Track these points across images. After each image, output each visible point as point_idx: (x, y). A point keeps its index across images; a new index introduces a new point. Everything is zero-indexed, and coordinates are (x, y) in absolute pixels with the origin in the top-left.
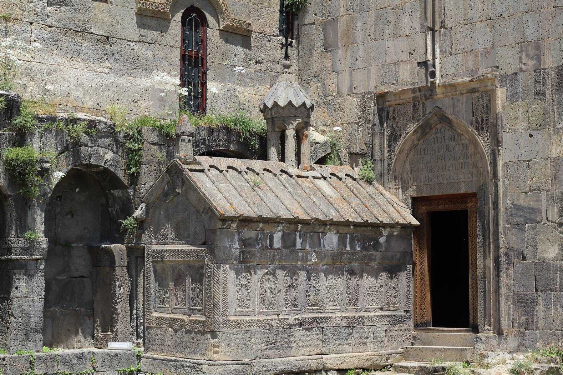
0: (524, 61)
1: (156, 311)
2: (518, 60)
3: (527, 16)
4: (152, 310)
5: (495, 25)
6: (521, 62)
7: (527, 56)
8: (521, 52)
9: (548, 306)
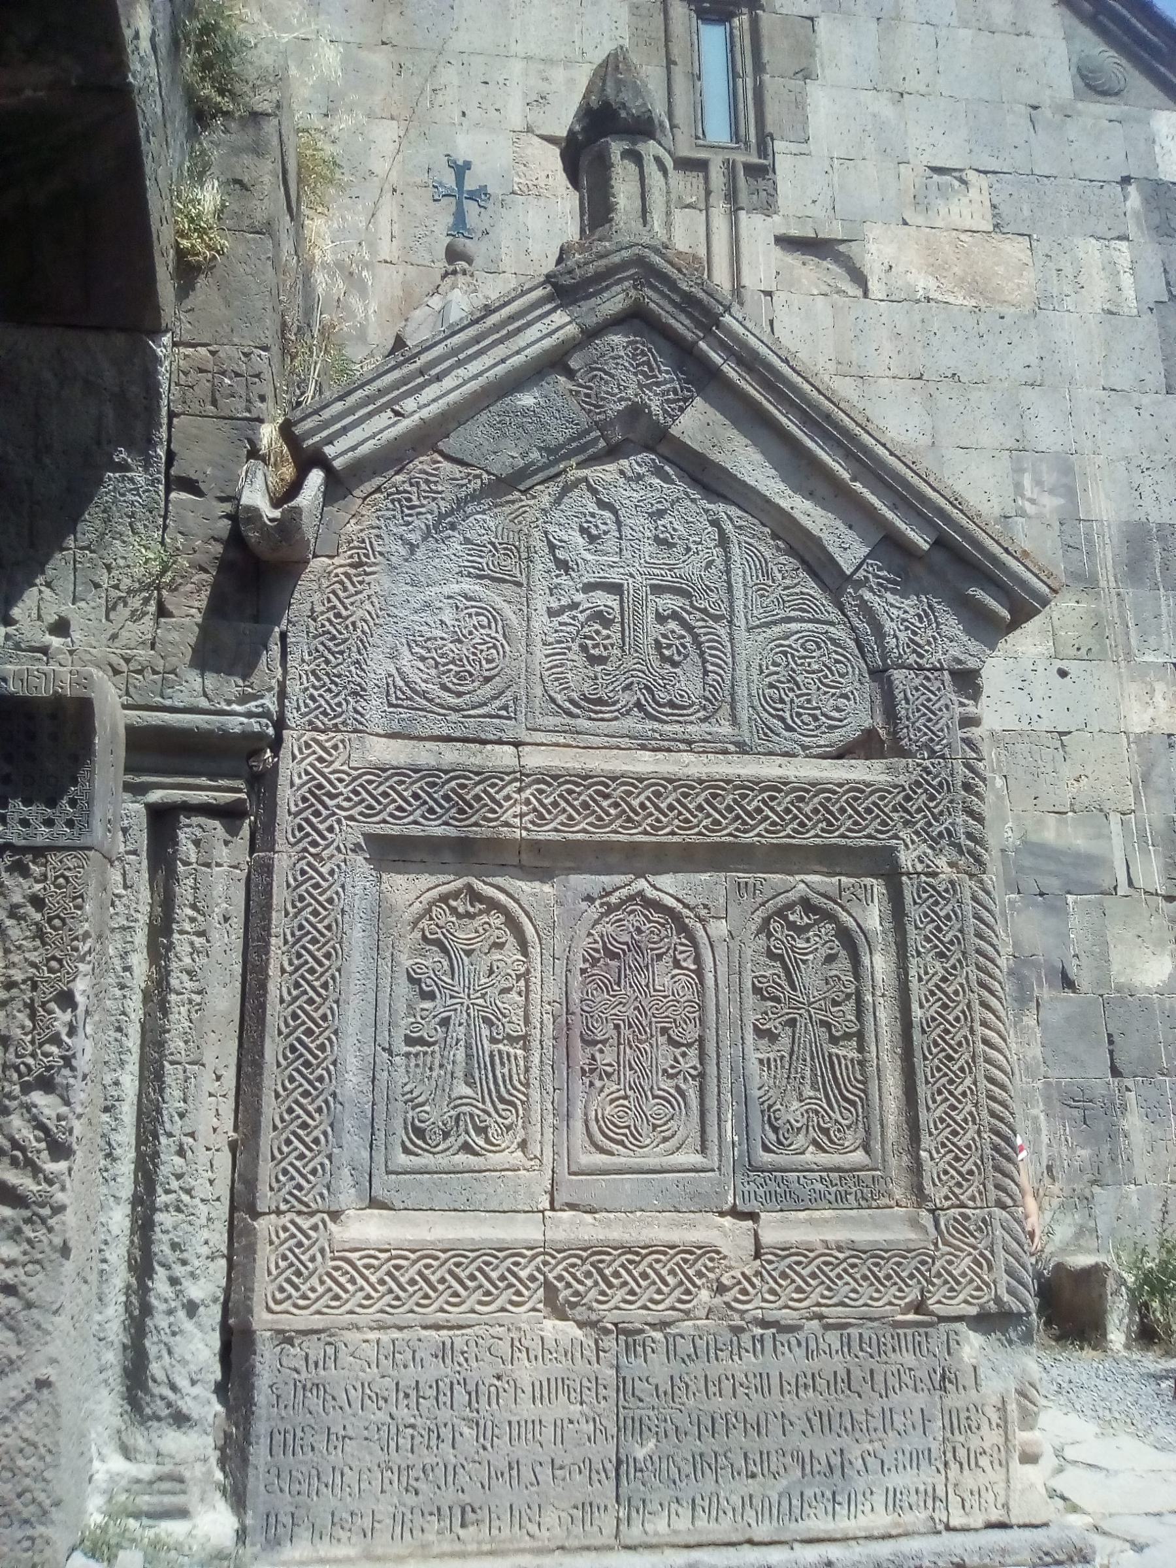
0: (1028, 494)
1: (374, 1203)
2: (1012, 488)
3: (1029, 396)
4: (347, 1196)
5: (936, 394)
6: (1023, 496)
7: (1038, 483)
9: (1154, 1114)
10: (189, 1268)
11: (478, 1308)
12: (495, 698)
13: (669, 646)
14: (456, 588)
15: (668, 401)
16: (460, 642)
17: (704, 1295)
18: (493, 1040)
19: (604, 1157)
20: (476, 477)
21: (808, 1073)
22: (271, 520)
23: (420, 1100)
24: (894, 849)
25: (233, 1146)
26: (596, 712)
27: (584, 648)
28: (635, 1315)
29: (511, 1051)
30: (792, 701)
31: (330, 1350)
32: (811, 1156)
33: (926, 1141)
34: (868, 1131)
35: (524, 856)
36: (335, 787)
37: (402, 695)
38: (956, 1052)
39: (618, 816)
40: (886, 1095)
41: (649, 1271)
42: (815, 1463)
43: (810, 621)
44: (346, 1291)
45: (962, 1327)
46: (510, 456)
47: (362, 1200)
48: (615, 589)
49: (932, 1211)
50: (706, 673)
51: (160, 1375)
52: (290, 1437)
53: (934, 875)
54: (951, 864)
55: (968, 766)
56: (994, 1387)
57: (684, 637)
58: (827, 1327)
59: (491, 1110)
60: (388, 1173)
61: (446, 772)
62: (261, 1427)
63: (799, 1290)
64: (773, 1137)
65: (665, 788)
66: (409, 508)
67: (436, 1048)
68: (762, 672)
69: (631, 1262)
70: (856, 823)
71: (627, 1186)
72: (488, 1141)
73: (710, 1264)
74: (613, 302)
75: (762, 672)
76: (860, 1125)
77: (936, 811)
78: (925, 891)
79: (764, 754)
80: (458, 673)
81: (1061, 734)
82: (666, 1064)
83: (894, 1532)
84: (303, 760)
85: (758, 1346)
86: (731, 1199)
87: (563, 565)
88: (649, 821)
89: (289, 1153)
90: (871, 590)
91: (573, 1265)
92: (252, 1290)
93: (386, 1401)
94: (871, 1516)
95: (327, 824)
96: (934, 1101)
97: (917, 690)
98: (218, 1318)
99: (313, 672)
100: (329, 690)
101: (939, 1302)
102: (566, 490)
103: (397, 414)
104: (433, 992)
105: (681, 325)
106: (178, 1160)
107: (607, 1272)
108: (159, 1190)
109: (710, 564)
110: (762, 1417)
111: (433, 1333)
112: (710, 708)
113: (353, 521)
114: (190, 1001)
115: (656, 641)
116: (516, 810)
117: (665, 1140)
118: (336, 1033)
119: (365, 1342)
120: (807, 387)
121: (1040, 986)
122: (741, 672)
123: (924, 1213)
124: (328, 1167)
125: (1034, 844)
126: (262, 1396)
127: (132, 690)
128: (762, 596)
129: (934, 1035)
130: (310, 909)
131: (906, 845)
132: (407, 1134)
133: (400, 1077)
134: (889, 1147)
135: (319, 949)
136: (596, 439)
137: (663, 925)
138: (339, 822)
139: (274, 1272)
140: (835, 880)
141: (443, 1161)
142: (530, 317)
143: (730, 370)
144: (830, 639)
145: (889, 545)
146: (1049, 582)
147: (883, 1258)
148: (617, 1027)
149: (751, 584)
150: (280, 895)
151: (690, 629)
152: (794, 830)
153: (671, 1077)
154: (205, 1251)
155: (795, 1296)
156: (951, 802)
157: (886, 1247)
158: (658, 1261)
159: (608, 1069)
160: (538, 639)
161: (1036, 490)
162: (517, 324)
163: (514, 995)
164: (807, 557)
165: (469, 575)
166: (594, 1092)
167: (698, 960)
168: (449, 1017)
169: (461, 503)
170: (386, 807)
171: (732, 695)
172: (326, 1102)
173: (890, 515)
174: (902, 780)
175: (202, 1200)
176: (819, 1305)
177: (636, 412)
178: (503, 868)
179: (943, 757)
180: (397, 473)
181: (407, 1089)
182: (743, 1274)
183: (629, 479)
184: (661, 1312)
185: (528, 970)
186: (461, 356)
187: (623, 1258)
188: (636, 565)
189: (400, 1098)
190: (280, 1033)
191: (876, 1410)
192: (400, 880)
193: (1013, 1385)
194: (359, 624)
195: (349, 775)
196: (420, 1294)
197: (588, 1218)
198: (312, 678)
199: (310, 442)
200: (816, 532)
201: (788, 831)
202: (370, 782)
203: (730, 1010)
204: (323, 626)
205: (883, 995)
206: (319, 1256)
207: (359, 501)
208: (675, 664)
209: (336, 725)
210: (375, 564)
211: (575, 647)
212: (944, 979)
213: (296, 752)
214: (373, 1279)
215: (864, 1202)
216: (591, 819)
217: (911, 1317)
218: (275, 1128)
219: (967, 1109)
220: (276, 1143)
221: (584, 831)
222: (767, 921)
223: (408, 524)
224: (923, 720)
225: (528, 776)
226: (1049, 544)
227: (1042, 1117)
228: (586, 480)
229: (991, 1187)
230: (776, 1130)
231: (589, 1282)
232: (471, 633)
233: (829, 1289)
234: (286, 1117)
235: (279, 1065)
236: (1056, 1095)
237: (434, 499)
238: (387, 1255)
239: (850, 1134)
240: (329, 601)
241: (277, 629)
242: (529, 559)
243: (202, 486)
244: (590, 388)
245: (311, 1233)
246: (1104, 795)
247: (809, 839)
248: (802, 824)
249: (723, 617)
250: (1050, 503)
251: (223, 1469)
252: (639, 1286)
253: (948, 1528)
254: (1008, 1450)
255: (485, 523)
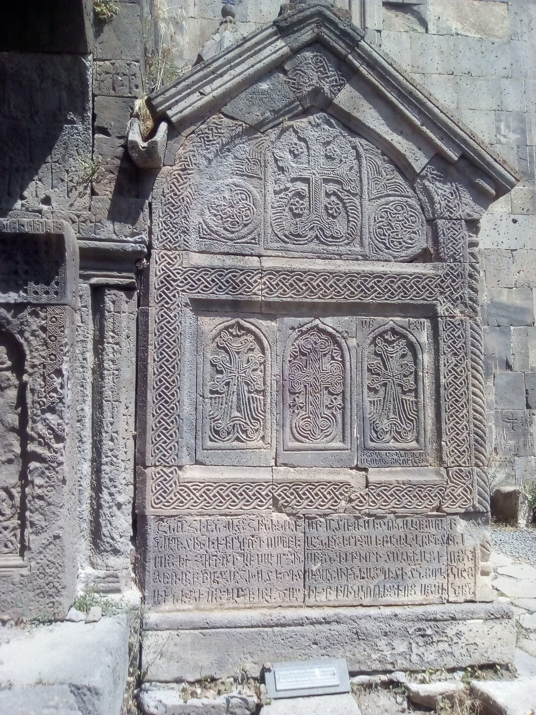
0: (503, 133)
1: (197, 462)
2: (495, 129)
3: (505, 83)
4: (185, 459)
5: (460, 82)
6: (500, 134)
7: (508, 127)
8: (499, 121)
10: (117, 489)
11: (244, 507)
12: (249, 234)
13: (332, 209)
14: (230, 181)
15: (333, 86)
16: (233, 207)
17: (343, 503)
18: (249, 392)
19: (299, 444)
20: (241, 125)
21: (392, 407)
22: (143, 148)
23: (217, 418)
24: (435, 305)
25: (135, 437)
26: (297, 241)
27: (291, 210)
28: (312, 511)
29: (257, 396)
30: (389, 235)
31: (180, 524)
32: (392, 444)
33: (444, 438)
34: (418, 433)
35: (263, 309)
36: (176, 277)
37: (206, 233)
38: (460, 398)
39: (307, 290)
40: (427, 417)
41: (319, 492)
42: (390, 573)
43: (399, 196)
44: (186, 499)
45: (457, 517)
46: (256, 115)
47: (192, 461)
48: (306, 180)
49: (446, 468)
50: (349, 221)
51: (107, 533)
52: (163, 560)
53: (453, 317)
54: (461, 312)
55: (471, 266)
56: (470, 543)
57: (338, 204)
58: (397, 517)
59: (249, 423)
60: (203, 449)
61: (227, 269)
62: (151, 555)
63: (385, 501)
64: (375, 435)
65: (329, 277)
66: (208, 141)
67: (224, 395)
68: (375, 221)
69: (311, 489)
70: (418, 293)
71: (309, 456)
72: (247, 436)
73: (346, 490)
74: (306, 35)
75: (375, 221)
76: (415, 430)
77: (455, 287)
78: (449, 325)
79: (375, 261)
80: (232, 222)
81: (512, 250)
82: (327, 403)
83: (424, 603)
84: (161, 264)
85: (367, 525)
86: (355, 462)
87: (281, 169)
88: (321, 292)
89: (159, 441)
90: (429, 180)
91: (285, 490)
92: (145, 498)
93: (204, 545)
94: (415, 596)
95: (172, 294)
96: (449, 420)
97: (449, 229)
98: (131, 510)
99: (165, 222)
100: (172, 231)
101: (448, 507)
102: (283, 131)
103: (202, 94)
104: (222, 371)
105: (340, 46)
106: (111, 443)
107: (300, 493)
108: (103, 456)
109: (351, 168)
110: (368, 554)
111: (224, 517)
112: (350, 238)
113: (181, 148)
114: (113, 374)
115: (326, 206)
116: (260, 287)
117: (326, 436)
118: (179, 388)
119: (194, 522)
120: (401, 78)
121: (496, 368)
122: (366, 222)
123: (442, 469)
124: (177, 447)
125: (496, 303)
126: (151, 542)
127: (81, 230)
128: (376, 184)
129: (450, 390)
130: (166, 333)
131: (441, 304)
132: (211, 433)
133: (208, 408)
134: (427, 440)
135: (170, 351)
136: (298, 106)
137: (327, 341)
138: (178, 293)
139: (154, 491)
140: (407, 320)
141: (227, 445)
142: (265, 43)
143: (364, 70)
144: (408, 205)
145: (438, 158)
146: (515, 176)
147: (423, 488)
148: (305, 386)
149: (371, 178)
150: (152, 326)
151: (341, 200)
152: (389, 297)
153: (329, 408)
154: (124, 482)
155: (384, 504)
156: (463, 283)
157: (425, 483)
158: (323, 488)
159: (301, 405)
160: (269, 206)
161: (507, 130)
162: (259, 47)
163: (258, 372)
164: (399, 165)
165: (237, 174)
166: (295, 415)
167: (342, 356)
168: (229, 382)
169: (233, 139)
170: (199, 285)
171: (361, 232)
172: (175, 418)
173: (439, 143)
174: (440, 272)
175: (122, 460)
176: (394, 507)
177: (317, 92)
178: (253, 314)
179: (460, 262)
180: (202, 124)
181: (211, 413)
182: (360, 494)
183: (313, 126)
184: (324, 510)
185: (265, 361)
186: (232, 64)
187: (307, 487)
188: (316, 168)
189: (208, 417)
190: (154, 388)
191: (418, 552)
192: (206, 319)
193: (479, 542)
194: (185, 199)
195: (182, 271)
196: (218, 501)
197: (292, 470)
198: (164, 225)
199: (160, 108)
200: (403, 151)
201: (386, 297)
202: (192, 274)
203: (357, 379)
204: (168, 199)
205: (427, 373)
206: (174, 485)
207: (184, 138)
208: (334, 217)
209: (175, 247)
210: (192, 169)
211: (287, 209)
212: (456, 365)
213: (158, 260)
214: (198, 495)
215: (416, 464)
216: (294, 291)
217: (435, 513)
218: (153, 430)
219: (464, 423)
220: (153, 437)
221: (291, 297)
222: (375, 339)
223: (207, 149)
224: (451, 244)
225: (265, 271)
226: (512, 157)
227: (493, 426)
228: (292, 126)
229: (473, 458)
230: (376, 432)
231: (292, 497)
232: (238, 203)
233: (399, 501)
234: (158, 425)
235: (154, 402)
236: (500, 417)
237: (220, 137)
238: (203, 485)
239: (410, 434)
240: (171, 187)
241: (147, 201)
242: (265, 166)
243: (110, 131)
244: (295, 80)
245: (170, 475)
246: (531, 280)
247: (395, 301)
248: (392, 294)
249: (357, 194)
250: (513, 137)
251: (135, 572)
252: (314, 499)
253: (448, 602)
254: (475, 570)
255: (244, 148)
